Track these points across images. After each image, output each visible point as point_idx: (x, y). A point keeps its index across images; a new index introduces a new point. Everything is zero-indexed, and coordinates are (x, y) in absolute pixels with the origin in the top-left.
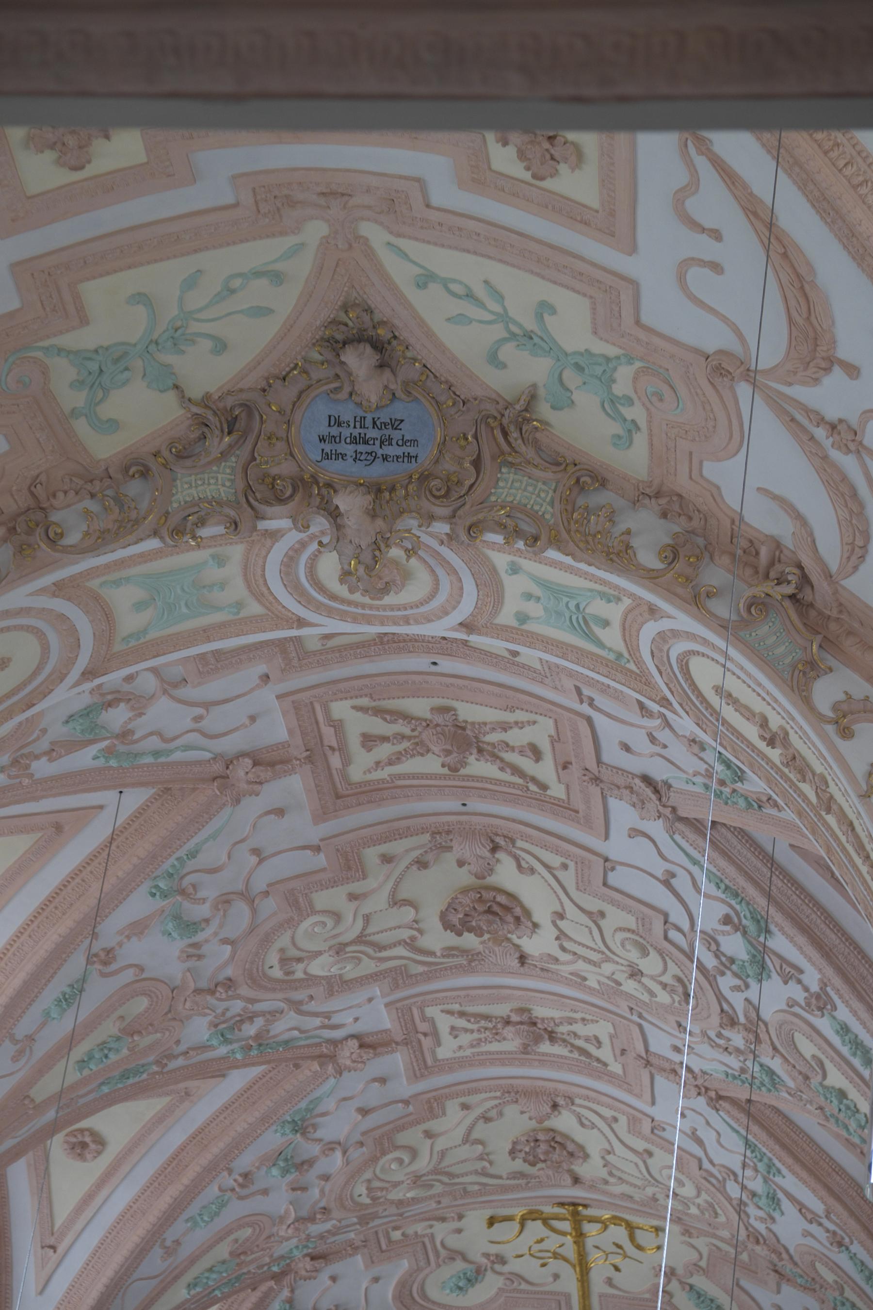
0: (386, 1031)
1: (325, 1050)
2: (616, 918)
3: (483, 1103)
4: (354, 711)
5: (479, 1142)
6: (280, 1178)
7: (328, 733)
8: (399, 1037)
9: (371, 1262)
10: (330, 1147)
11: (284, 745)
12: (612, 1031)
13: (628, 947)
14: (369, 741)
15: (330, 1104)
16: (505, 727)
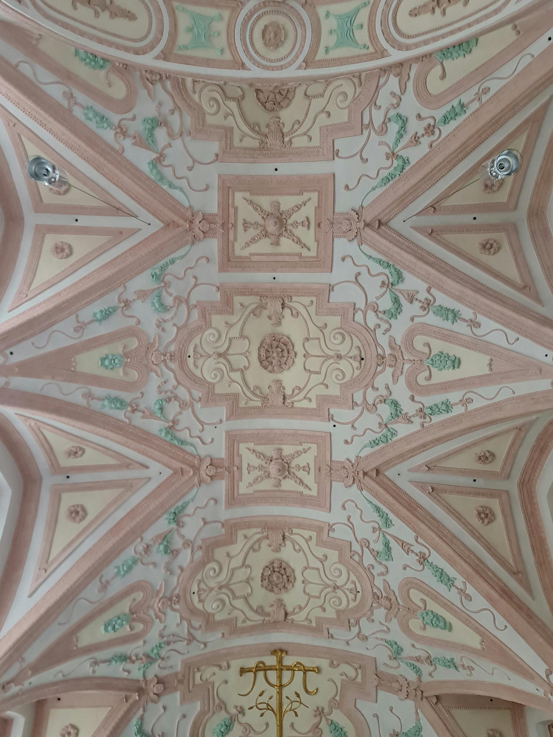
0: (222, 459)
1: (196, 462)
2: (334, 321)
3: (254, 533)
4: (243, 200)
5: (249, 566)
6: (163, 552)
7: (232, 211)
8: (226, 465)
9: (183, 700)
10: (187, 544)
11: (215, 215)
12: (316, 454)
13: (337, 336)
14: (246, 225)
15: (190, 510)
16: (298, 207)
